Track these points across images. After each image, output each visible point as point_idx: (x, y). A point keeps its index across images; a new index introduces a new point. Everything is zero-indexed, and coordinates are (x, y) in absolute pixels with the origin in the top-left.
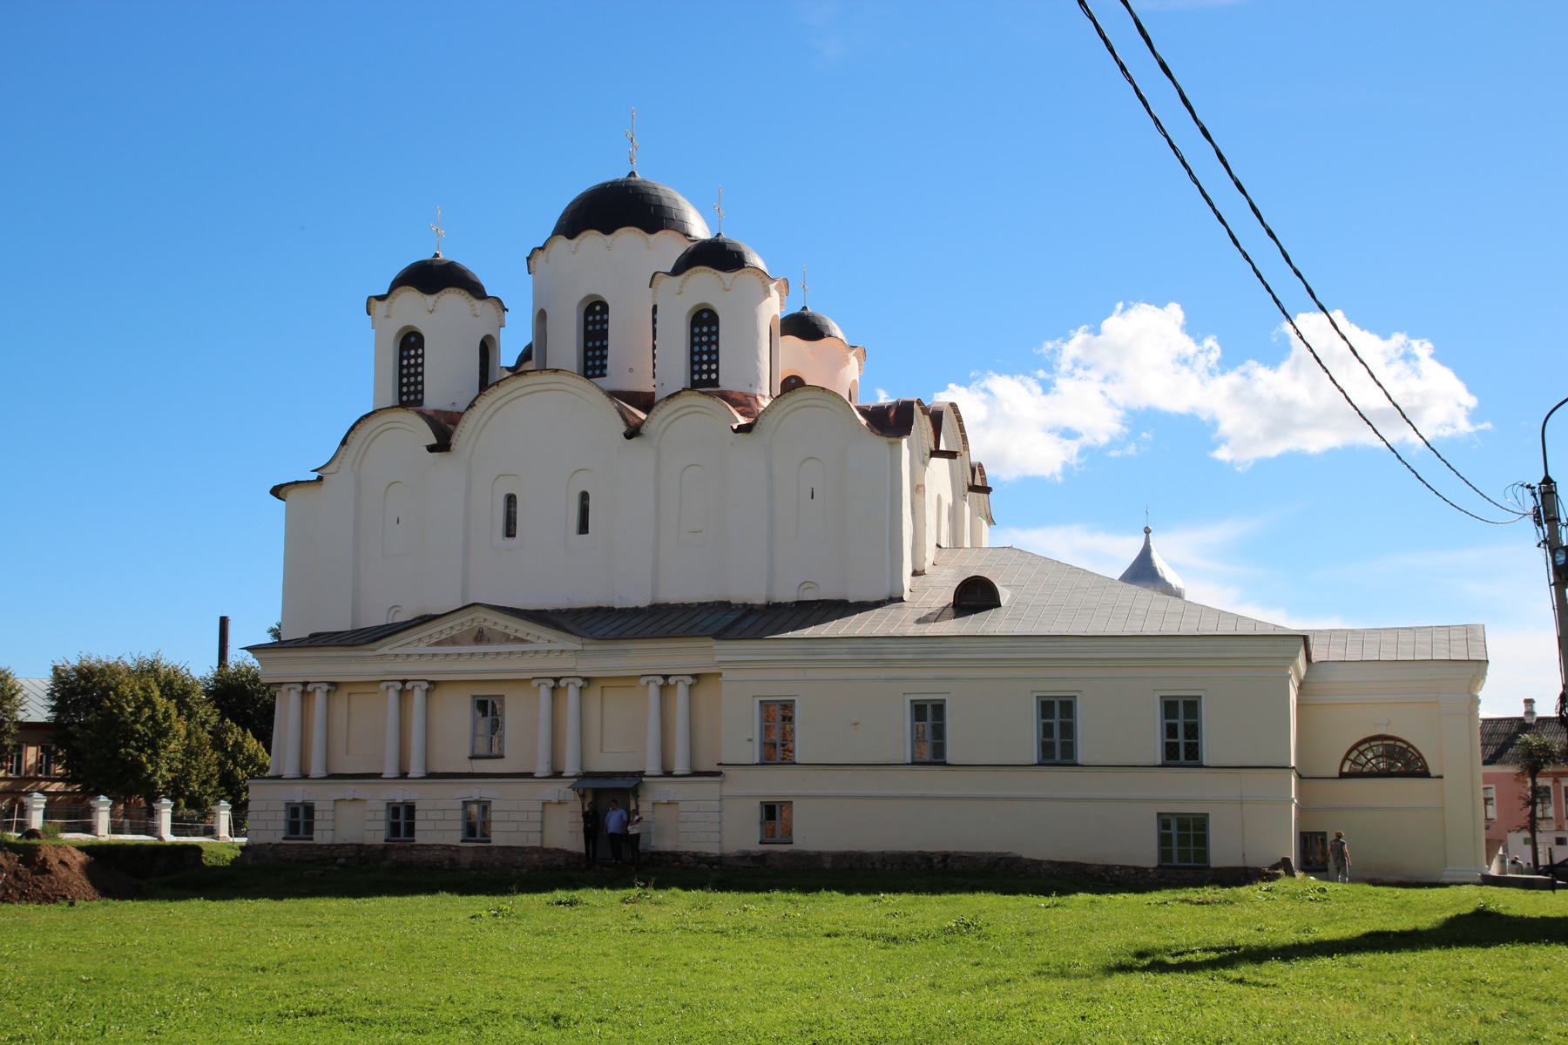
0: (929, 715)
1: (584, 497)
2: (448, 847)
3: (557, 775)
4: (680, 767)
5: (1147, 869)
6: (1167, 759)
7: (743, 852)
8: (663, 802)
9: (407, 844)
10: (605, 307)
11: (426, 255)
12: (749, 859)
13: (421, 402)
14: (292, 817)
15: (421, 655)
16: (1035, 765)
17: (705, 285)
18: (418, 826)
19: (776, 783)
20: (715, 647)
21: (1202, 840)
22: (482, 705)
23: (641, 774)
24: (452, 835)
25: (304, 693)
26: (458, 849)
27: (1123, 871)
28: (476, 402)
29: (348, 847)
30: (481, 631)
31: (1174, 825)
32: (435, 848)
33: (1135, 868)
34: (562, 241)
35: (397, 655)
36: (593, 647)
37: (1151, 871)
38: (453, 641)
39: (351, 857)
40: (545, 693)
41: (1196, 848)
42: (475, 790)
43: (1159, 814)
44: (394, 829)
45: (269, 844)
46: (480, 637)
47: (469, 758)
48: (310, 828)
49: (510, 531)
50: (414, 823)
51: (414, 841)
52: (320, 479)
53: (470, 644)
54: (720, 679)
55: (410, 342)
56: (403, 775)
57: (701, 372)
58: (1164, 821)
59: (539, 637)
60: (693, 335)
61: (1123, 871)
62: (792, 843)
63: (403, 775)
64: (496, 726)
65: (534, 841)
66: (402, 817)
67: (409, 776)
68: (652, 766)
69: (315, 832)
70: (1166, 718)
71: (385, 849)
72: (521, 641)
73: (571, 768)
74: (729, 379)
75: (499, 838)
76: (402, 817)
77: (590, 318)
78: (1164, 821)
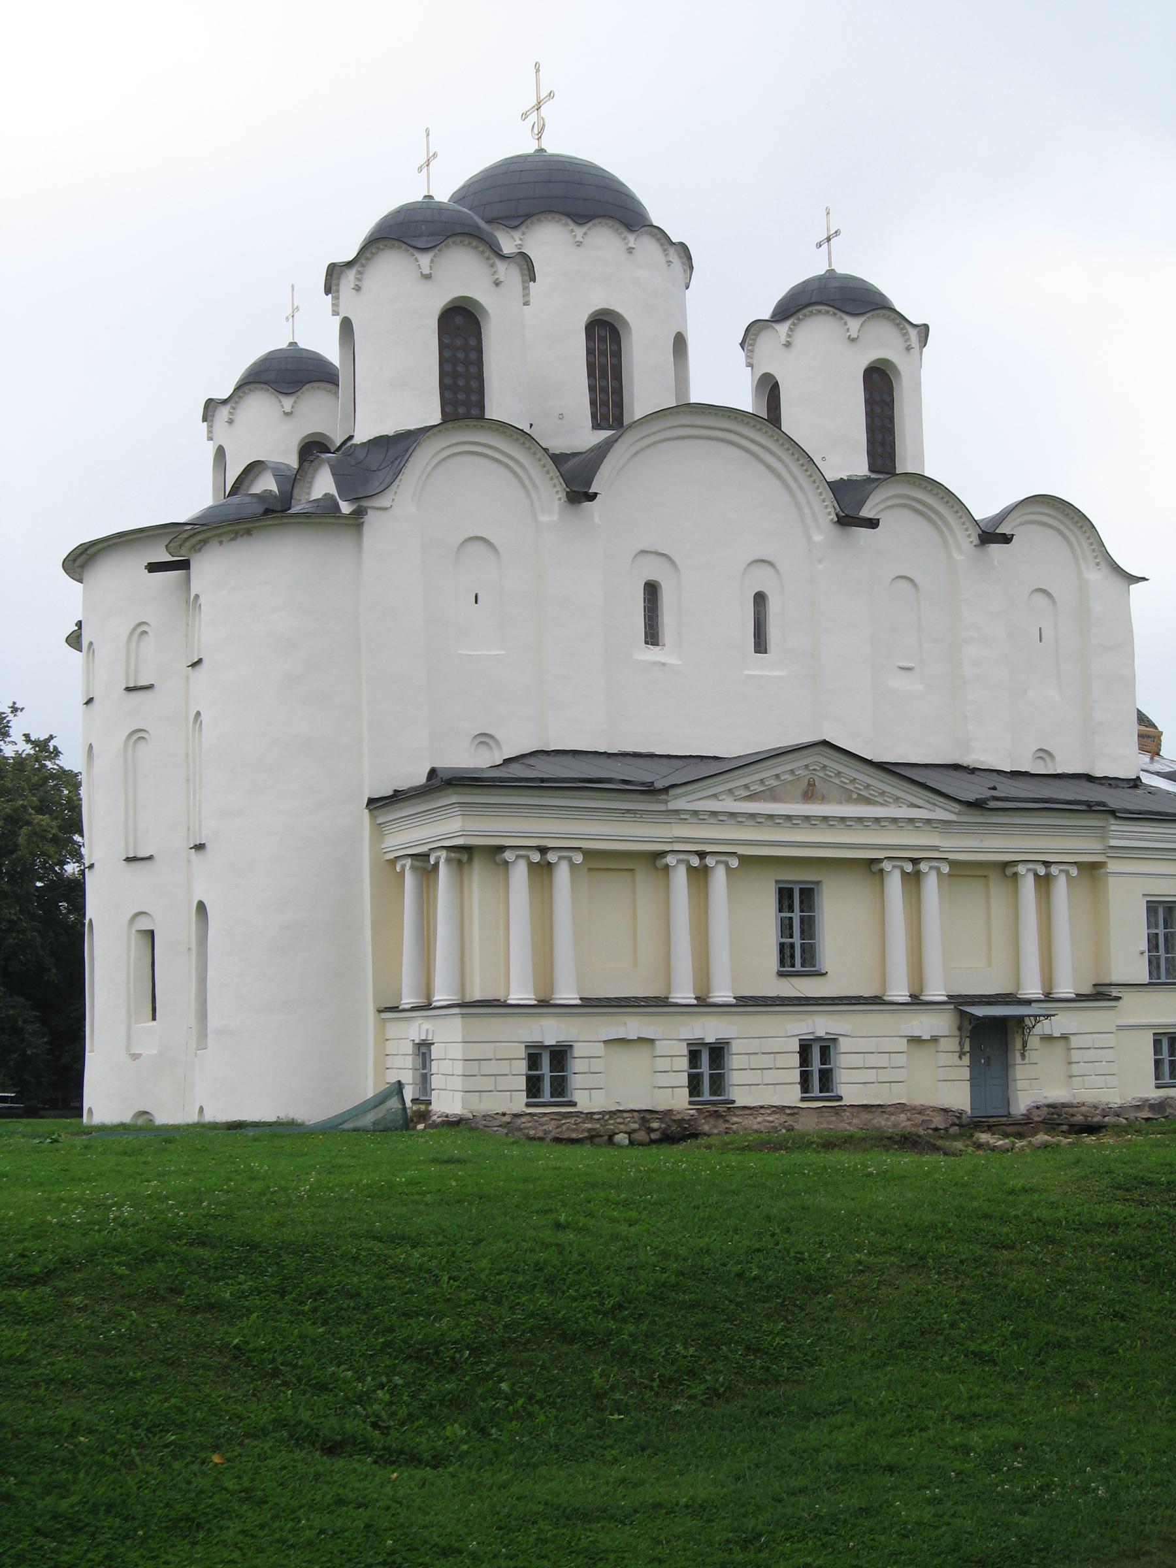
1: (760, 599)
3: (916, 1001)
7: (1141, 1099)
8: (1055, 1035)
9: (721, 1109)
12: (1147, 1109)
14: (530, 1068)
20: (1113, 828)
22: (785, 896)
26: (794, 1111)
29: (626, 1115)
30: (811, 784)
32: (762, 1111)
38: (771, 795)
39: (634, 1131)
42: (820, 1025)
45: (504, 1114)
46: (809, 794)
48: (560, 1087)
56: (703, 1003)
63: (703, 1003)
64: (808, 927)
68: (1032, 989)
72: (868, 801)
73: (936, 991)
74: (905, 465)
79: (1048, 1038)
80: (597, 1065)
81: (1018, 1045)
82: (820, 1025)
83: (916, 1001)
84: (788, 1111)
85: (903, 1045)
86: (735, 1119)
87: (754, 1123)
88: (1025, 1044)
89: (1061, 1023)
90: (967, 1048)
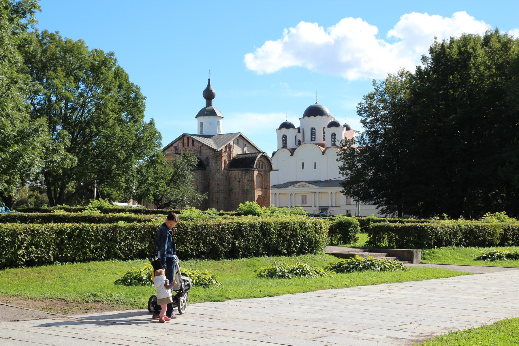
1: (315, 163)
3: (315, 207)
4: (334, 205)
10: (315, 129)
11: (284, 121)
13: (287, 147)
17: (333, 129)
23: (328, 206)
25: (275, 195)
34: (306, 118)
36: (321, 188)
46: (303, 186)
49: (303, 168)
55: (285, 138)
57: (333, 143)
64: (305, 199)
68: (330, 205)
72: (309, 187)
73: (318, 206)
89: (332, 208)
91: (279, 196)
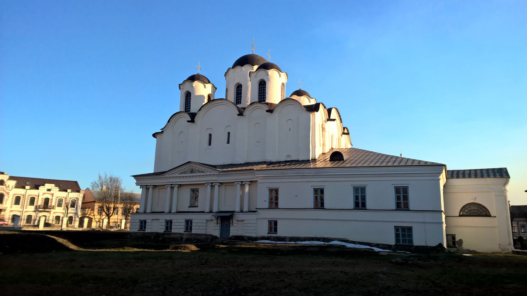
0: (319, 193)
1: (229, 133)
2: (180, 233)
3: (211, 212)
4: (246, 209)
5: (391, 245)
6: (397, 208)
9: (170, 233)
10: (241, 85)
13: (190, 111)
15: (176, 177)
16: (353, 209)
18: (173, 227)
19: (273, 214)
21: (411, 236)
22: (193, 191)
23: (234, 211)
24: (182, 231)
25: (147, 188)
26: (183, 234)
27: (383, 246)
28: (202, 109)
30: (192, 170)
31: (400, 230)
33: (387, 245)
35: (170, 177)
37: (393, 246)
38: (185, 173)
40: (209, 188)
41: (407, 237)
42: (189, 217)
43: (395, 227)
44: (167, 228)
45: (134, 232)
46: (192, 171)
47: (189, 207)
49: (210, 144)
50: (172, 226)
51: (171, 232)
52: (162, 132)
53: (189, 173)
54: (257, 182)
56: (170, 212)
58: (397, 228)
59: (207, 171)
60: (259, 88)
61: (383, 246)
62: (277, 234)
64: (196, 198)
65: (204, 232)
66: (169, 224)
67: (171, 212)
68: (238, 209)
69: (146, 229)
70: (397, 193)
71: (164, 234)
72: (203, 172)
73: (215, 209)
75: (194, 231)
76: (169, 224)
77: (238, 89)
78: (397, 228)
79: (238, 221)
80: (150, 224)
81: (231, 222)
82: (189, 217)
83: (211, 212)
84: (182, 234)
85: (205, 221)
86: (171, 235)
87: (174, 236)
88: (232, 222)
89: (241, 217)
90: (219, 222)
91: (153, 191)
